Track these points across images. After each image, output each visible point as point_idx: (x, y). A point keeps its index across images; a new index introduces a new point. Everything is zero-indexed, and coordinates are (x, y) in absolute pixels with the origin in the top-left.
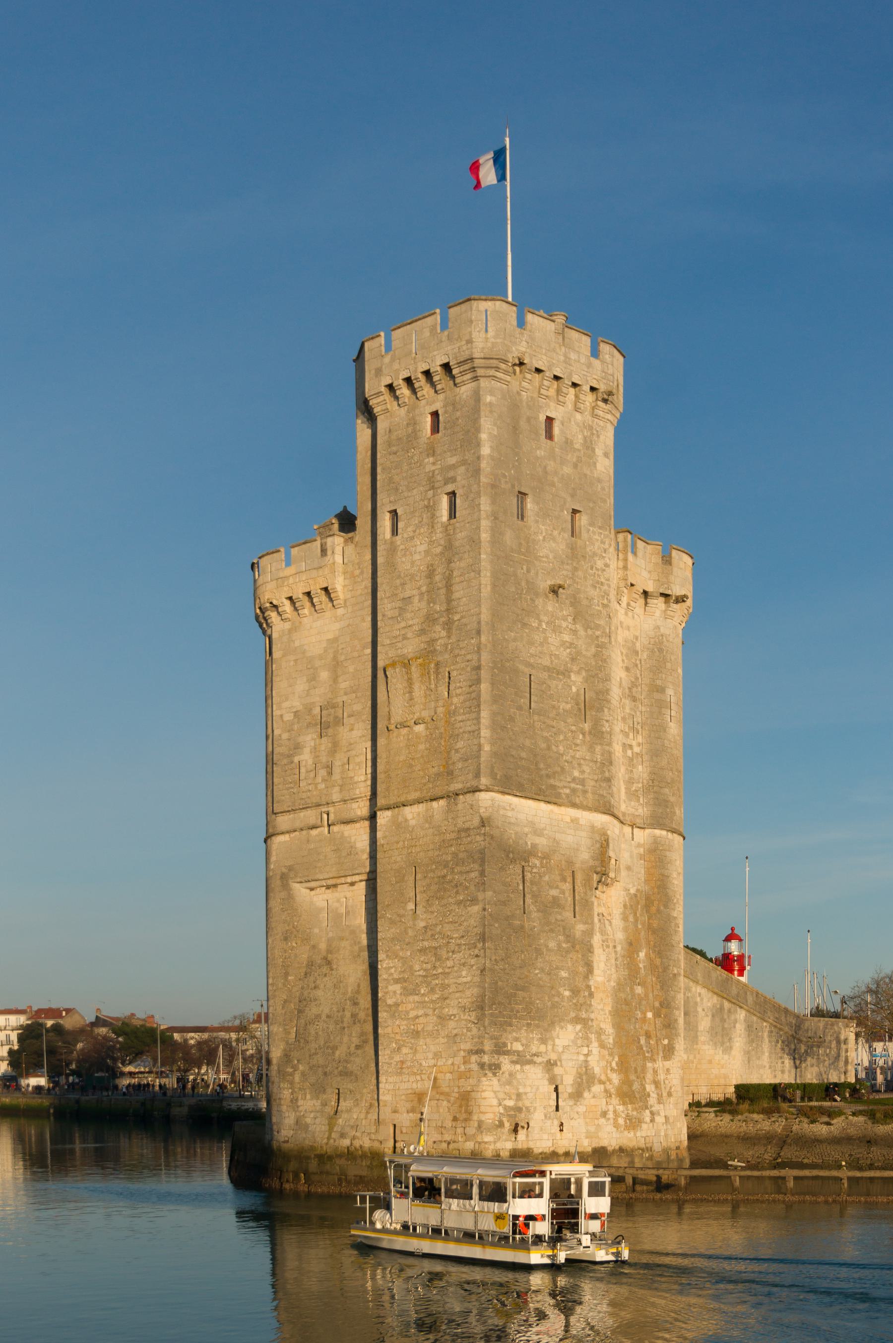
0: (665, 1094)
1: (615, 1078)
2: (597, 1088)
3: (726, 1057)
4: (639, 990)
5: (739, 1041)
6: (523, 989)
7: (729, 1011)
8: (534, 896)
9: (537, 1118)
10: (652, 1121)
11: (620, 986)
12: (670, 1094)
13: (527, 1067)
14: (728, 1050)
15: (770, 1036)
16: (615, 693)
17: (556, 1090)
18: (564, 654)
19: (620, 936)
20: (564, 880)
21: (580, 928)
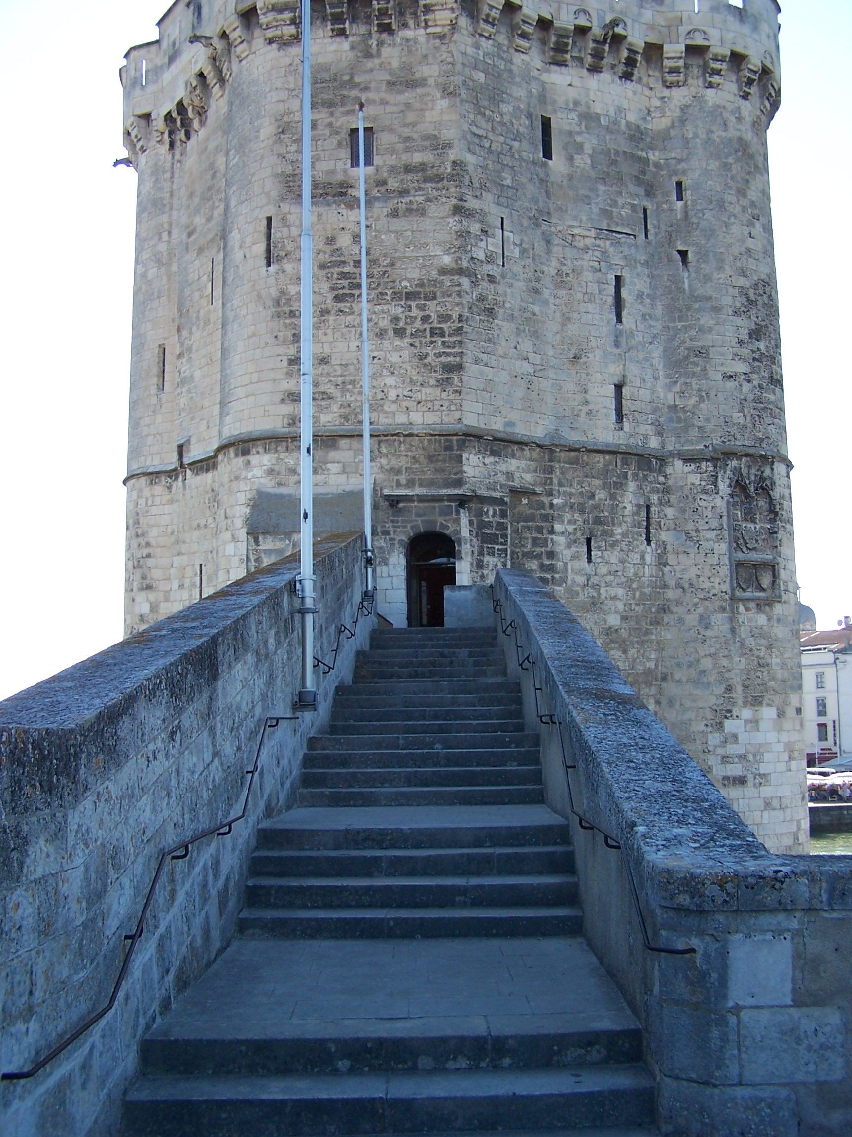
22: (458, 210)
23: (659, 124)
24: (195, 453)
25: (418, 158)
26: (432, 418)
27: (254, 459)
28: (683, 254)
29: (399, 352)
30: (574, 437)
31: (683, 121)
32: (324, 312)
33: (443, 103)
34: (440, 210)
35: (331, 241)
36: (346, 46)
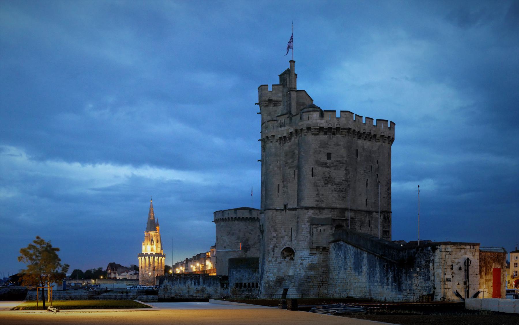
3: (360, 277)
5: (365, 269)
7: (361, 253)
14: (360, 273)
15: (380, 264)
22: (346, 170)
23: (374, 149)
24: (289, 207)
25: (339, 159)
26: (341, 206)
27: (310, 211)
28: (377, 175)
29: (335, 194)
30: (360, 208)
31: (379, 149)
32: (323, 186)
33: (343, 149)
34: (343, 169)
35: (324, 173)
36: (326, 136)
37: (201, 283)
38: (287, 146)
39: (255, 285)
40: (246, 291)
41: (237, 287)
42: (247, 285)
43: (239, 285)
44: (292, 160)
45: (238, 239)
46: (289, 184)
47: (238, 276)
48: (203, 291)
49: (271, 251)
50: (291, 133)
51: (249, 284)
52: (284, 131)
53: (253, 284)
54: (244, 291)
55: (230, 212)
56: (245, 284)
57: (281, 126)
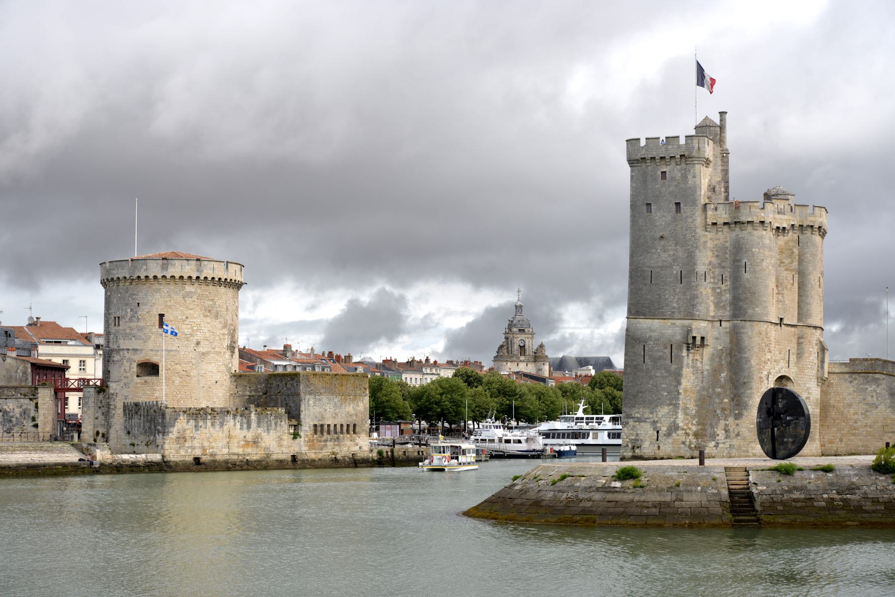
0: (732, 435)
1: (694, 428)
2: (680, 432)
4: (719, 390)
6: (641, 392)
8: (650, 356)
9: (646, 444)
10: (716, 446)
11: (703, 388)
12: (738, 435)
13: (642, 424)
16: (701, 268)
17: (658, 432)
18: (670, 260)
19: (707, 367)
20: (666, 348)
21: (673, 367)
37: (254, 425)
38: (782, 240)
39: (345, 428)
40: (331, 441)
41: (316, 433)
42: (332, 428)
43: (319, 429)
44: (789, 260)
45: (225, 327)
46: (785, 292)
47: (317, 409)
48: (255, 442)
49: (765, 379)
50: (793, 225)
51: (335, 425)
52: (784, 221)
53: (342, 425)
54: (326, 441)
55: (216, 265)
56: (329, 425)
57: (778, 213)
